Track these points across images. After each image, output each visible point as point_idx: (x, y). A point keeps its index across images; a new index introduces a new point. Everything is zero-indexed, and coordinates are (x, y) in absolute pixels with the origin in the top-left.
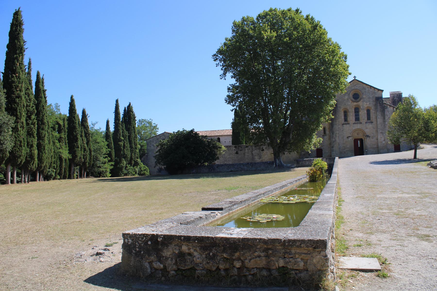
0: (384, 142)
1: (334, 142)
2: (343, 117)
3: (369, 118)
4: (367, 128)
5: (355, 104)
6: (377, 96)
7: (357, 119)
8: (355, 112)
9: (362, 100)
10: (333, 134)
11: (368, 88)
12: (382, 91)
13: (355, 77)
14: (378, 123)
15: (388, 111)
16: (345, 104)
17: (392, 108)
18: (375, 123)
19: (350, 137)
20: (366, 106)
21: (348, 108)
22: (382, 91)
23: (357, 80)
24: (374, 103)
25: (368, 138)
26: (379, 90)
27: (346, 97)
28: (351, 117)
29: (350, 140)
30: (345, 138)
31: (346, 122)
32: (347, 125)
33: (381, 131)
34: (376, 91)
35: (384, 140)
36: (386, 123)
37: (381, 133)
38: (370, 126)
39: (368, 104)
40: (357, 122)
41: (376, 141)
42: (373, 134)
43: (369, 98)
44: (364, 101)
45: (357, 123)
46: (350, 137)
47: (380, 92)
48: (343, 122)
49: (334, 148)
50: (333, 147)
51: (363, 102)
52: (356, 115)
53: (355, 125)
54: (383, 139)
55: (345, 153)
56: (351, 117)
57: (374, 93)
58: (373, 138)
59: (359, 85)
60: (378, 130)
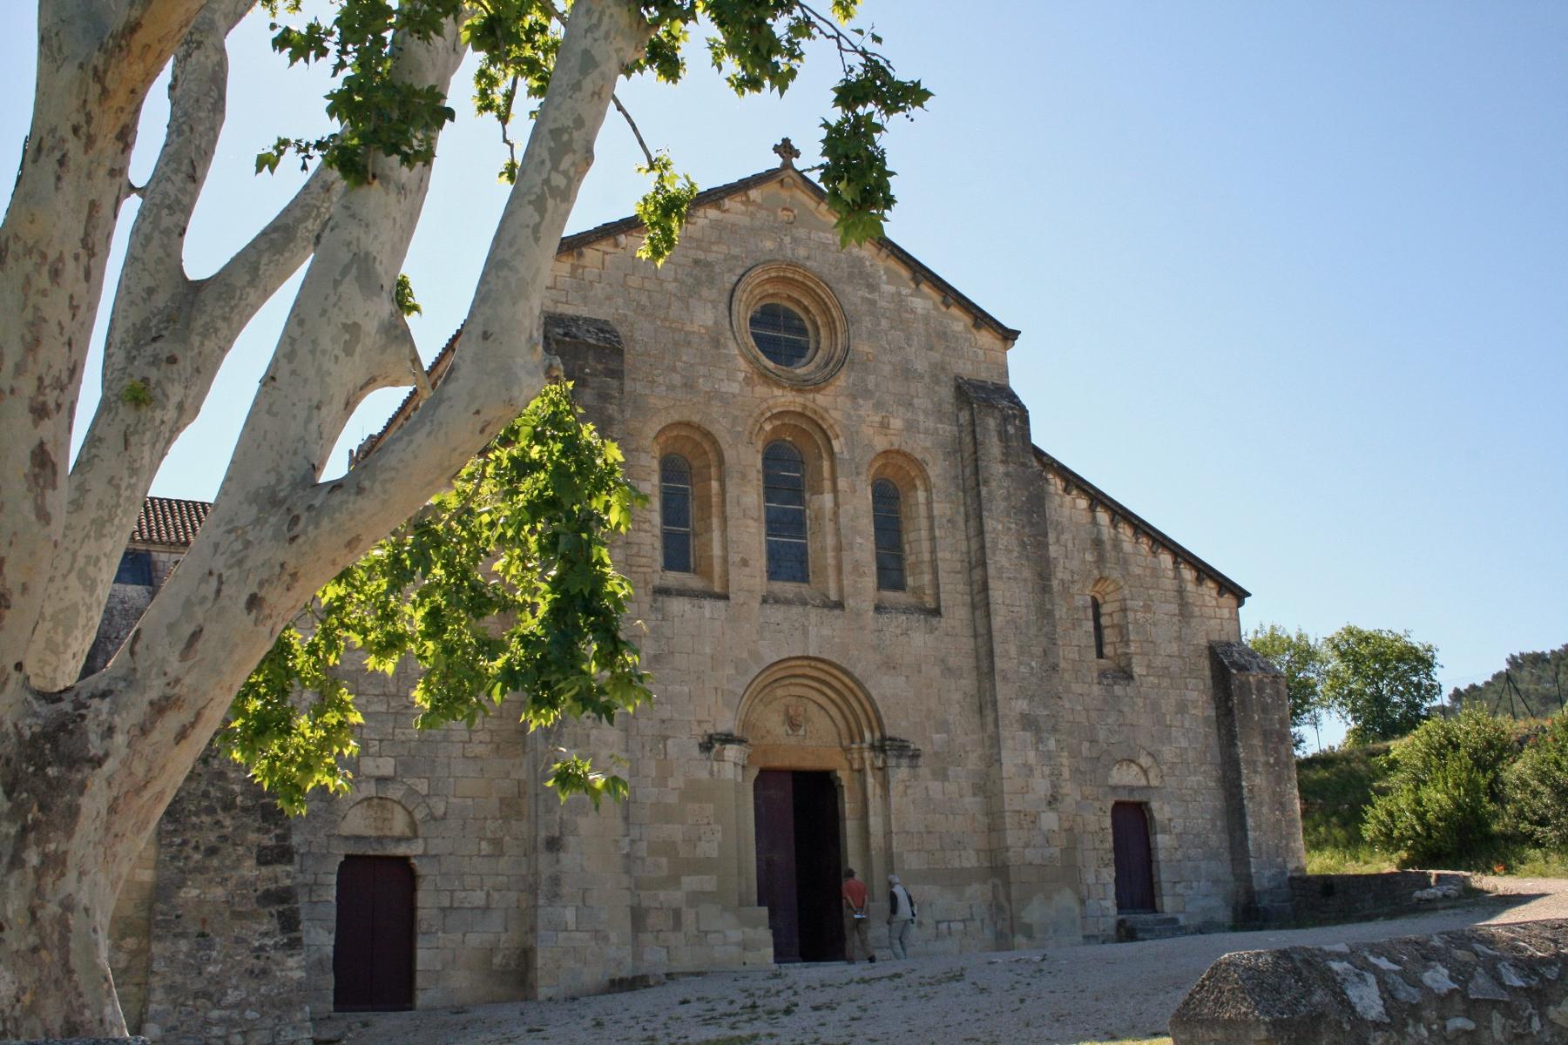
0: (1049, 820)
3: (891, 572)
4: (890, 666)
5: (785, 399)
6: (966, 369)
8: (772, 488)
9: (842, 380)
11: (893, 278)
12: (1009, 336)
14: (998, 621)
16: (689, 386)
18: (957, 615)
19: (728, 739)
20: (880, 444)
21: (720, 429)
22: (1009, 336)
24: (947, 430)
25: (900, 773)
26: (981, 319)
27: (705, 317)
28: (740, 528)
30: (684, 745)
32: (708, 604)
33: (1022, 705)
35: (1053, 801)
37: (1028, 722)
39: (897, 423)
40: (788, 588)
41: (971, 802)
42: (943, 726)
43: (906, 373)
44: (867, 394)
46: (728, 739)
47: (986, 338)
49: (569, 859)
50: (554, 844)
51: (854, 397)
52: (775, 524)
53: (777, 614)
54: (1041, 787)
55: (677, 915)
56: (740, 528)
57: (943, 335)
58: (941, 775)
60: (1002, 690)
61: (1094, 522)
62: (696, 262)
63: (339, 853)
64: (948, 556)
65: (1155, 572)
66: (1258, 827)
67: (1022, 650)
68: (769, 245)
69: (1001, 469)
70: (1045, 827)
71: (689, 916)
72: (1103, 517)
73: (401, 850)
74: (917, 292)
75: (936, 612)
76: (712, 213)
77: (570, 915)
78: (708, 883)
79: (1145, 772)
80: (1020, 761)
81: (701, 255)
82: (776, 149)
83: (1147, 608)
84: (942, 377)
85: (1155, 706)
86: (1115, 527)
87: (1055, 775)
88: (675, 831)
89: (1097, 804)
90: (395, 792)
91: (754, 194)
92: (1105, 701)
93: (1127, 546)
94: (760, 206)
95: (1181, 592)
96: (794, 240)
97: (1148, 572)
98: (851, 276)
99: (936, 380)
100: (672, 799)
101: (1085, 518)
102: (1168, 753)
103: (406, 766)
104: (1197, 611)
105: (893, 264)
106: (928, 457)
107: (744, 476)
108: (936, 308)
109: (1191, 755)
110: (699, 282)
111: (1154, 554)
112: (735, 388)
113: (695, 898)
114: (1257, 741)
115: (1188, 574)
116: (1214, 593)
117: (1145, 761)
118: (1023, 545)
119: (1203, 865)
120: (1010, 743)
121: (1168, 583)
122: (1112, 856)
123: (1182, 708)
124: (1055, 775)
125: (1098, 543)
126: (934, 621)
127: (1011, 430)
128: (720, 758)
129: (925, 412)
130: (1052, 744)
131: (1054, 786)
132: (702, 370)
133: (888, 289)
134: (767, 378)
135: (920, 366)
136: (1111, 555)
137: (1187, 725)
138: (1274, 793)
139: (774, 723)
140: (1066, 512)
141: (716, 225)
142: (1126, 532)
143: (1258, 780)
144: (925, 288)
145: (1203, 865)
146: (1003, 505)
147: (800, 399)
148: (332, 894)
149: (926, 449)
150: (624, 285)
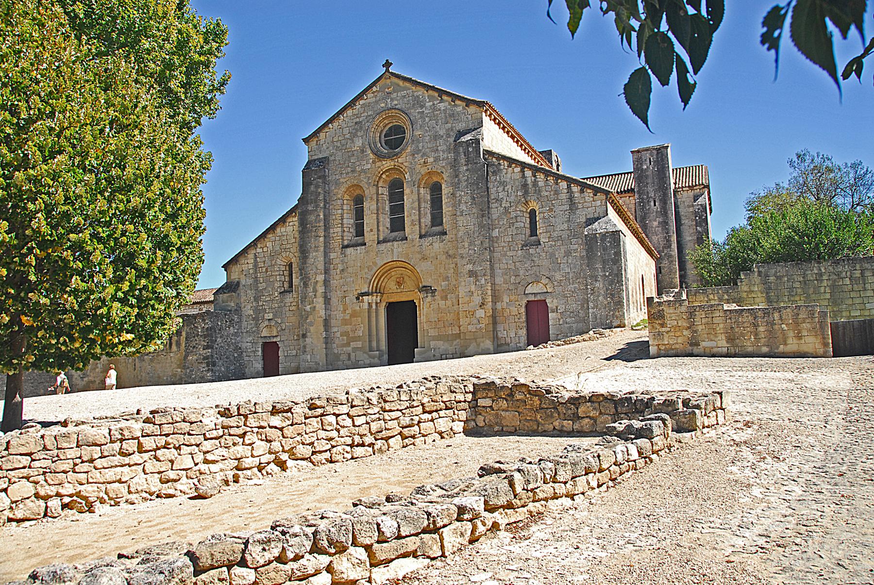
0: (480, 313)
1: (308, 314)
2: (349, 221)
4: (424, 258)
5: (387, 164)
7: (397, 225)
10: (306, 285)
11: (431, 98)
13: (388, 64)
15: (503, 184)
17: (519, 169)
19: (363, 294)
20: (424, 170)
23: (392, 73)
26: (469, 102)
27: (359, 142)
29: (366, 306)
30: (351, 297)
31: (359, 239)
33: (470, 267)
34: (460, 109)
35: (482, 305)
36: (495, 233)
37: (471, 274)
38: (436, 246)
39: (431, 160)
43: (436, 137)
45: (394, 240)
46: (363, 294)
47: (472, 109)
48: (349, 237)
50: (304, 336)
53: (383, 247)
54: (477, 300)
55: (349, 354)
58: (445, 298)
59: (404, 93)
61: (524, 176)
62: (356, 123)
63: (261, 341)
64: (450, 209)
65: (557, 193)
66: (595, 307)
67: (470, 244)
68: (383, 105)
69: (465, 168)
70: (478, 316)
71: (353, 355)
72: (528, 173)
73: (274, 340)
74: (442, 101)
75: (445, 234)
76: (362, 102)
77: (309, 357)
78: (359, 344)
79: (545, 285)
80: (467, 290)
81: (358, 120)
82: (383, 66)
83: (551, 210)
84: (452, 133)
85: (552, 255)
86: (535, 176)
87: (484, 294)
88: (348, 328)
89: (517, 303)
90: (273, 323)
91: (374, 89)
92: (524, 257)
93: (541, 184)
94: (378, 92)
95: (571, 198)
96: (392, 100)
97: (552, 193)
98: (414, 105)
99: (448, 136)
100: (348, 317)
101: (518, 176)
102: (558, 276)
103: (275, 316)
104: (580, 206)
105: (430, 92)
106: (444, 170)
107: (371, 198)
108: (450, 104)
109: (571, 275)
110: (357, 130)
111: (557, 184)
112: (369, 166)
113: (355, 349)
114: (599, 266)
115: (575, 189)
116: (591, 195)
117: (544, 281)
118: (473, 198)
119: (574, 326)
120: (463, 283)
121: (564, 196)
122: (525, 325)
123: (568, 253)
124: (484, 294)
125: (525, 186)
126: (444, 237)
127: (470, 149)
128: (363, 301)
129: (443, 151)
130: (483, 282)
131: (483, 299)
132: (358, 163)
133: (429, 104)
134: (380, 156)
135: (441, 133)
136: (531, 189)
137: (570, 261)
138: (607, 290)
139: (392, 286)
140: (509, 176)
141: (363, 106)
142: (541, 176)
143: (597, 285)
144: (445, 98)
145: (574, 326)
146: (465, 184)
147: (392, 163)
148: (260, 353)
149: (443, 167)
150: (333, 142)
